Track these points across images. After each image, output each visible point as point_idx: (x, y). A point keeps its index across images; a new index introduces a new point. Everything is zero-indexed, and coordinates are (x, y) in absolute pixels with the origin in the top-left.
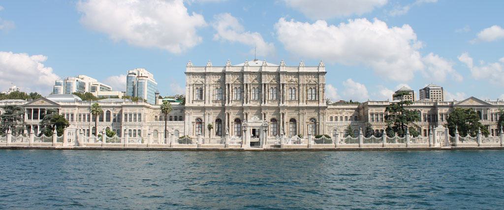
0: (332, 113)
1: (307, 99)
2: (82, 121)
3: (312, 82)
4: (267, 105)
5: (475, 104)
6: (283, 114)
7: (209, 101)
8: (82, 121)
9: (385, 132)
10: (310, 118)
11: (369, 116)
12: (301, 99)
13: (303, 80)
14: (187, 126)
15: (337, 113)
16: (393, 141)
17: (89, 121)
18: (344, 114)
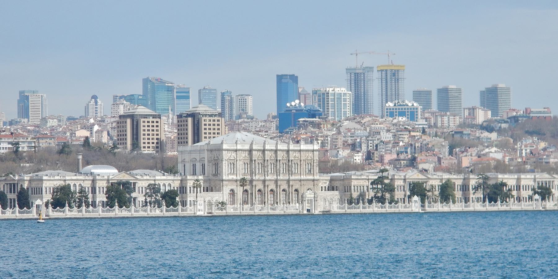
3: (309, 158)
4: (281, 178)
5: (420, 178)
6: (292, 186)
11: (353, 188)
13: (304, 156)
14: (225, 196)
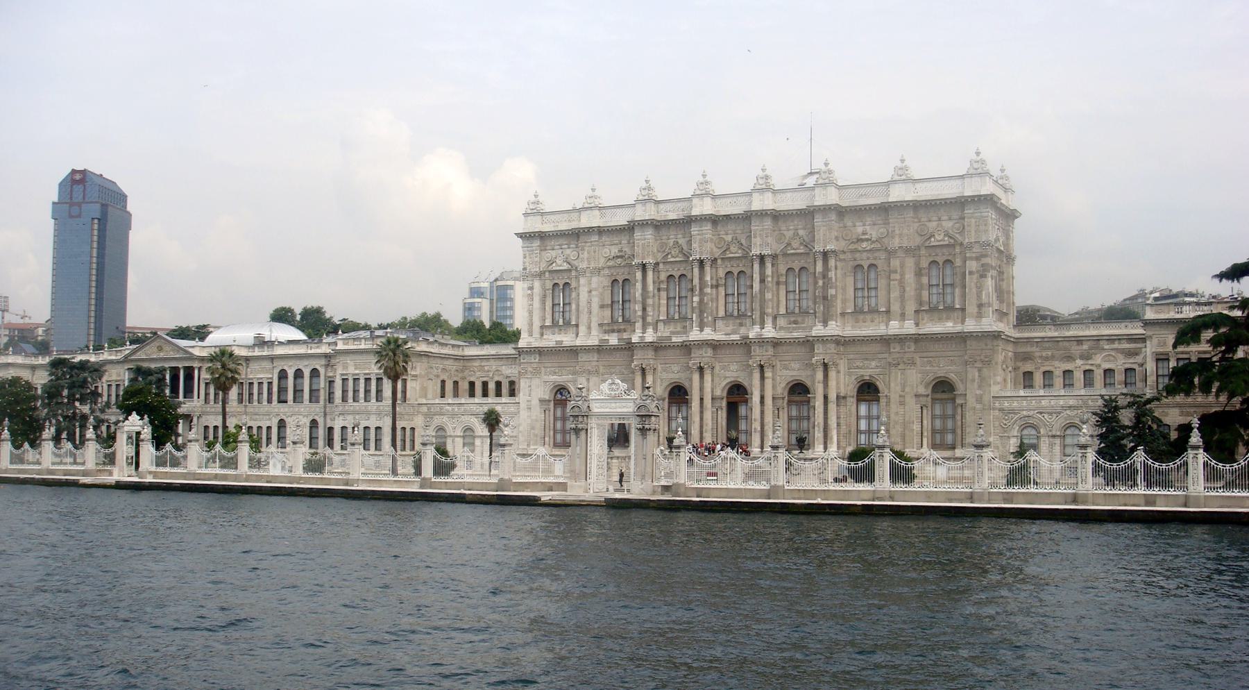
0: (1053, 357)
1: (921, 304)
2: (256, 403)
3: (939, 239)
4: (769, 332)
7: (589, 328)
8: (256, 403)
9: (1195, 438)
10: (931, 377)
12: (895, 307)
15: (1070, 358)
16: (1129, 477)
17: (270, 401)
18: (1100, 362)
